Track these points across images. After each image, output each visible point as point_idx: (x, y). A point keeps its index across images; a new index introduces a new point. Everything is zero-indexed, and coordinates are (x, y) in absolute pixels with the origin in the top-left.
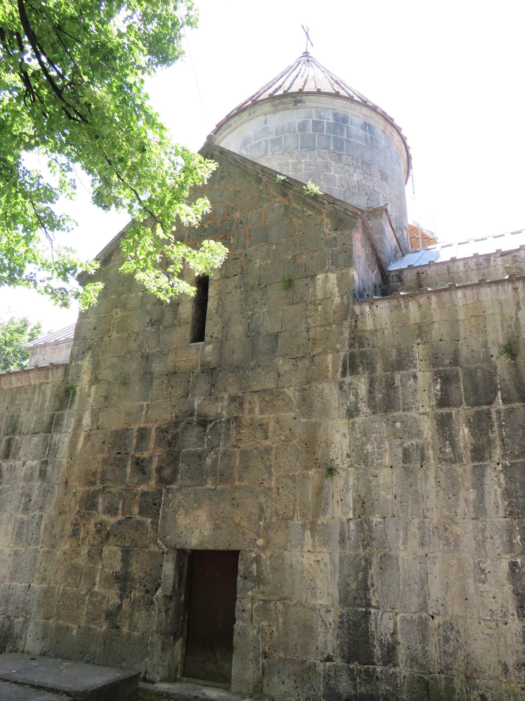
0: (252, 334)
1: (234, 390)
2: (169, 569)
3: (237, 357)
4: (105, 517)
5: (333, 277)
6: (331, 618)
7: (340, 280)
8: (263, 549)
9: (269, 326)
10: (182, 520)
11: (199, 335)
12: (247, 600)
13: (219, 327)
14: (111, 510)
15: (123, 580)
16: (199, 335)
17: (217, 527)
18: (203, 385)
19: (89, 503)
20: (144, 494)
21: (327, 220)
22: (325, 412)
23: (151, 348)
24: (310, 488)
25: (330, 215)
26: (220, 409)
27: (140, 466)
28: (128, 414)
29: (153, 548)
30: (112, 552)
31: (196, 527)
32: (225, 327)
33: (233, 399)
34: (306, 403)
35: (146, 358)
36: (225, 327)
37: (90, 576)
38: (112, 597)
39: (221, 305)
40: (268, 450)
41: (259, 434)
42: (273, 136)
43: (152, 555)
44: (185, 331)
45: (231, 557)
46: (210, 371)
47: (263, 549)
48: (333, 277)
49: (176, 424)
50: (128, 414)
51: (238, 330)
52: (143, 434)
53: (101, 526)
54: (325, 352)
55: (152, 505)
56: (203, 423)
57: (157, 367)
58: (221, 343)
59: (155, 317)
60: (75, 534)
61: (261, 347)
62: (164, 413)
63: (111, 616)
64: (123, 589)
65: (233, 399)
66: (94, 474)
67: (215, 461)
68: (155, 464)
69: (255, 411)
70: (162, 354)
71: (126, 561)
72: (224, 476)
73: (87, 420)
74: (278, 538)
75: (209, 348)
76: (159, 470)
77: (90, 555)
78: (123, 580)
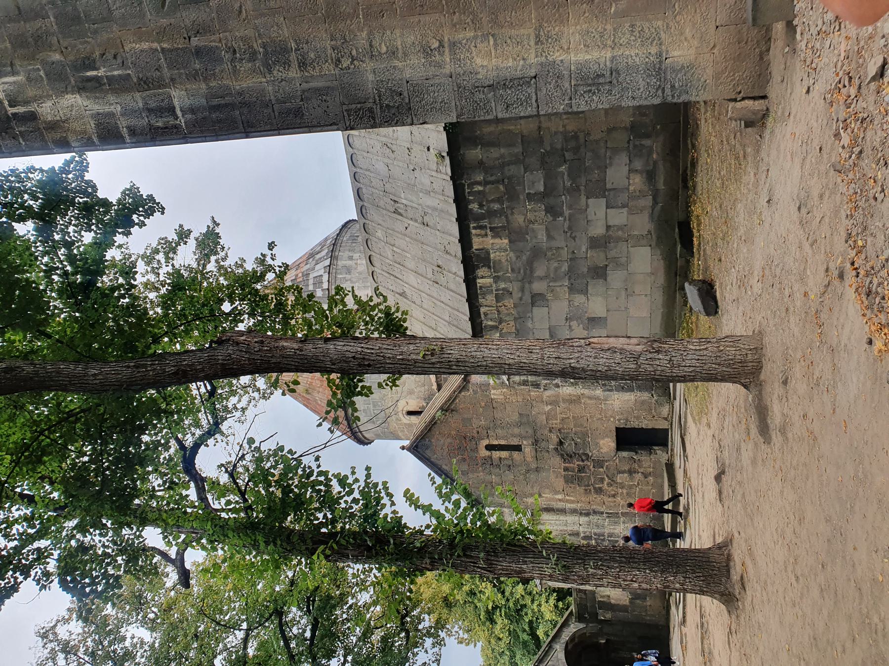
0: (520, 424)
1: (546, 432)
2: (625, 454)
3: (530, 431)
4: (605, 483)
5: (493, 392)
6: (639, 394)
7: (494, 389)
8: (615, 418)
9: (515, 417)
10: (604, 450)
11: (518, 448)
12: (635, 424)
13: (515, 439)
14: (602, 480)
15: (631, 472)
16: (518, 448)
17: (607, 436)
18: (543, 444)
19: (599, 491)
20: (594, 467)
21: (463, 393)
22: (558, 396)
23: (523, 469)
24: (589, 401)
25: (460, 392)
26: (554, 438)
27: (581, 469)
28: (557, 477)
29: (617, 461)
30: (619, 478)
31: (608, 444)
32: (513, 435)
33: (550, 431)
34: (554, 402)
35: (528, 471)
36: (513, 435)
37: (630, 487)
38: (639, 476)
39: (503, 438)
40: (573, 417)
41: (567, 420)
42: (371, 406)
43: (620, 461)
44: (516, 454)
45: (618, 430)
46: (536, 442)
47: (615, 418)
48: (493, 392)
49: (562, 456)
50: (557, 477)
51: (516, 431)
52: (566, 469)
53: (609, 485)
54: (530, 395)
55: (599, 463)
56: (561, 443)
57: (534, 466)
58: (521, 437)
59: (506, 468)
60: (614, 496)
61: (525, 420)
62: (556, 461)
63: (646, 476)
64: (635, 472)
65: (550, 431)
66: (586, 490)
67: (579, 438)
68: (581, 463)
69: (556, 423)
70: (528, 464)
71: (623, 472)
72: (585, 435)
73: (560, 497)
74: (610, 413)
75: (525, 442)
76: (583, 461)
77: (622, 488)
78: (631, 472)
